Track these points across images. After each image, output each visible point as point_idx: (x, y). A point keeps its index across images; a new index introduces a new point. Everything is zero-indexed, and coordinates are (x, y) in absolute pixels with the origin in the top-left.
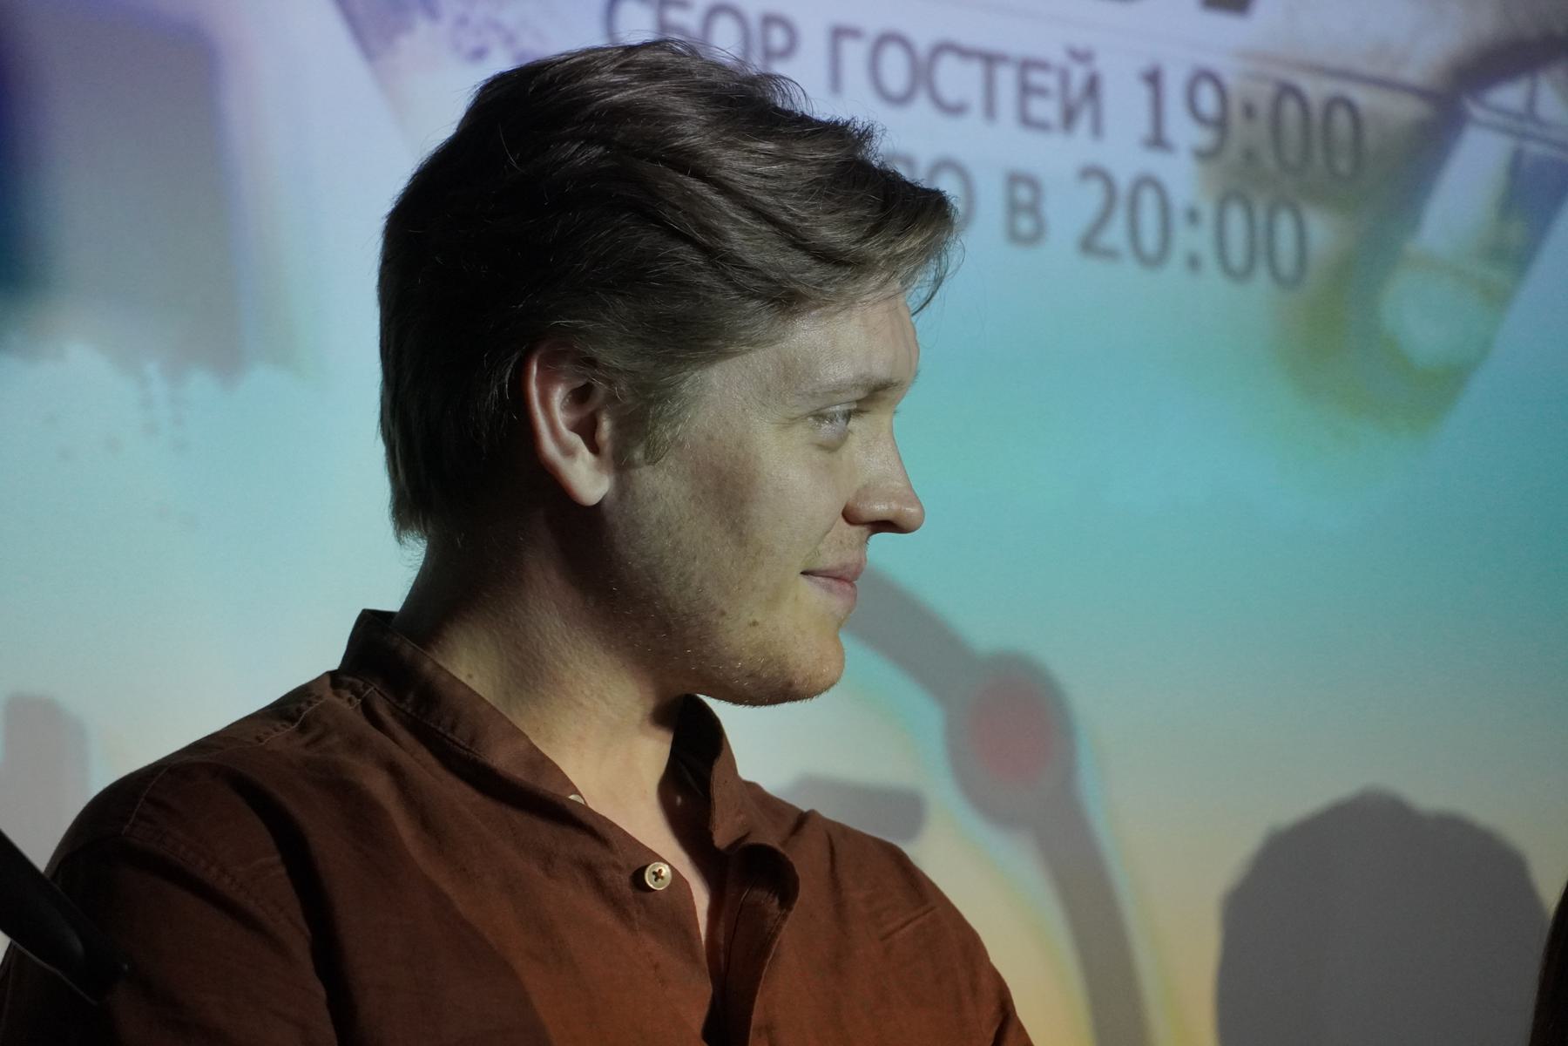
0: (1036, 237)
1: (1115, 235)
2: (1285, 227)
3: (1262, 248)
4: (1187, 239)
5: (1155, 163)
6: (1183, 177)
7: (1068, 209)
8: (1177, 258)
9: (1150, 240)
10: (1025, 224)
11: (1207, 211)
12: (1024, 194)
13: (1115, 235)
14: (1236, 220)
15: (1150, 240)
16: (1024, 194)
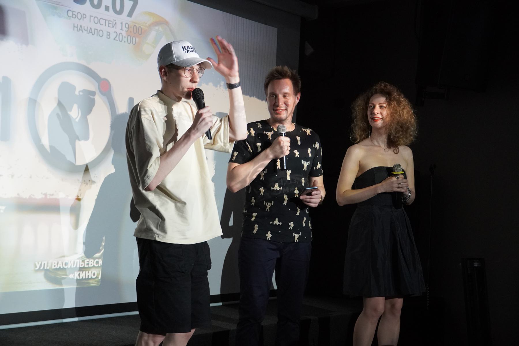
0: (109, 38)
1: (117, 38)
2: (134, 38)
3: (131, 41)
4: (124, 39)
5: (121, 32)
6: (124, 33)
7: (113, 36)
8: (123, 41)
9: (121, 40)
10: (108, 37)
11: (126, 37)
12: (108, 34)
13: (117, 38)
14: (129, 37)
15: (121, 40)
16: (108, 34)
